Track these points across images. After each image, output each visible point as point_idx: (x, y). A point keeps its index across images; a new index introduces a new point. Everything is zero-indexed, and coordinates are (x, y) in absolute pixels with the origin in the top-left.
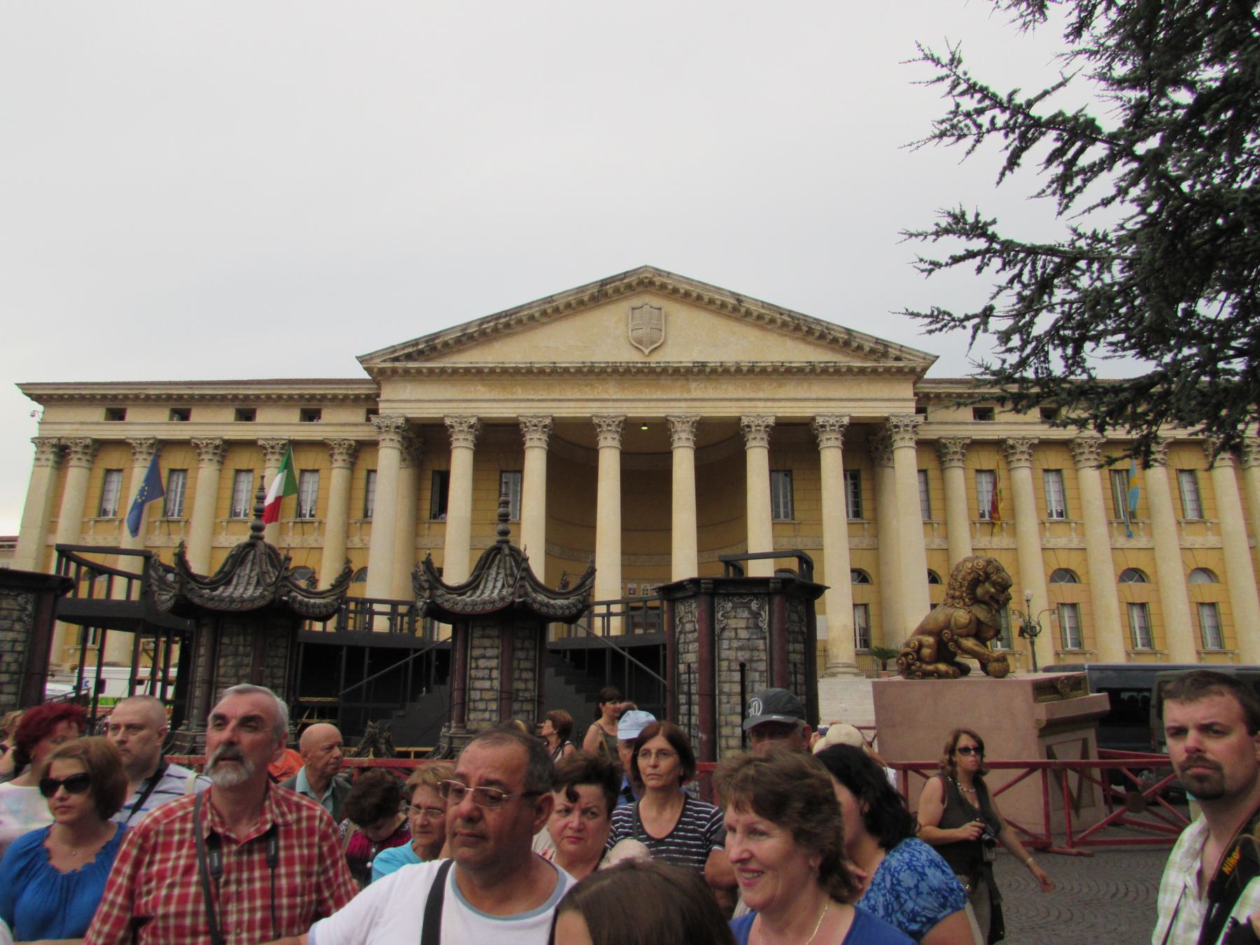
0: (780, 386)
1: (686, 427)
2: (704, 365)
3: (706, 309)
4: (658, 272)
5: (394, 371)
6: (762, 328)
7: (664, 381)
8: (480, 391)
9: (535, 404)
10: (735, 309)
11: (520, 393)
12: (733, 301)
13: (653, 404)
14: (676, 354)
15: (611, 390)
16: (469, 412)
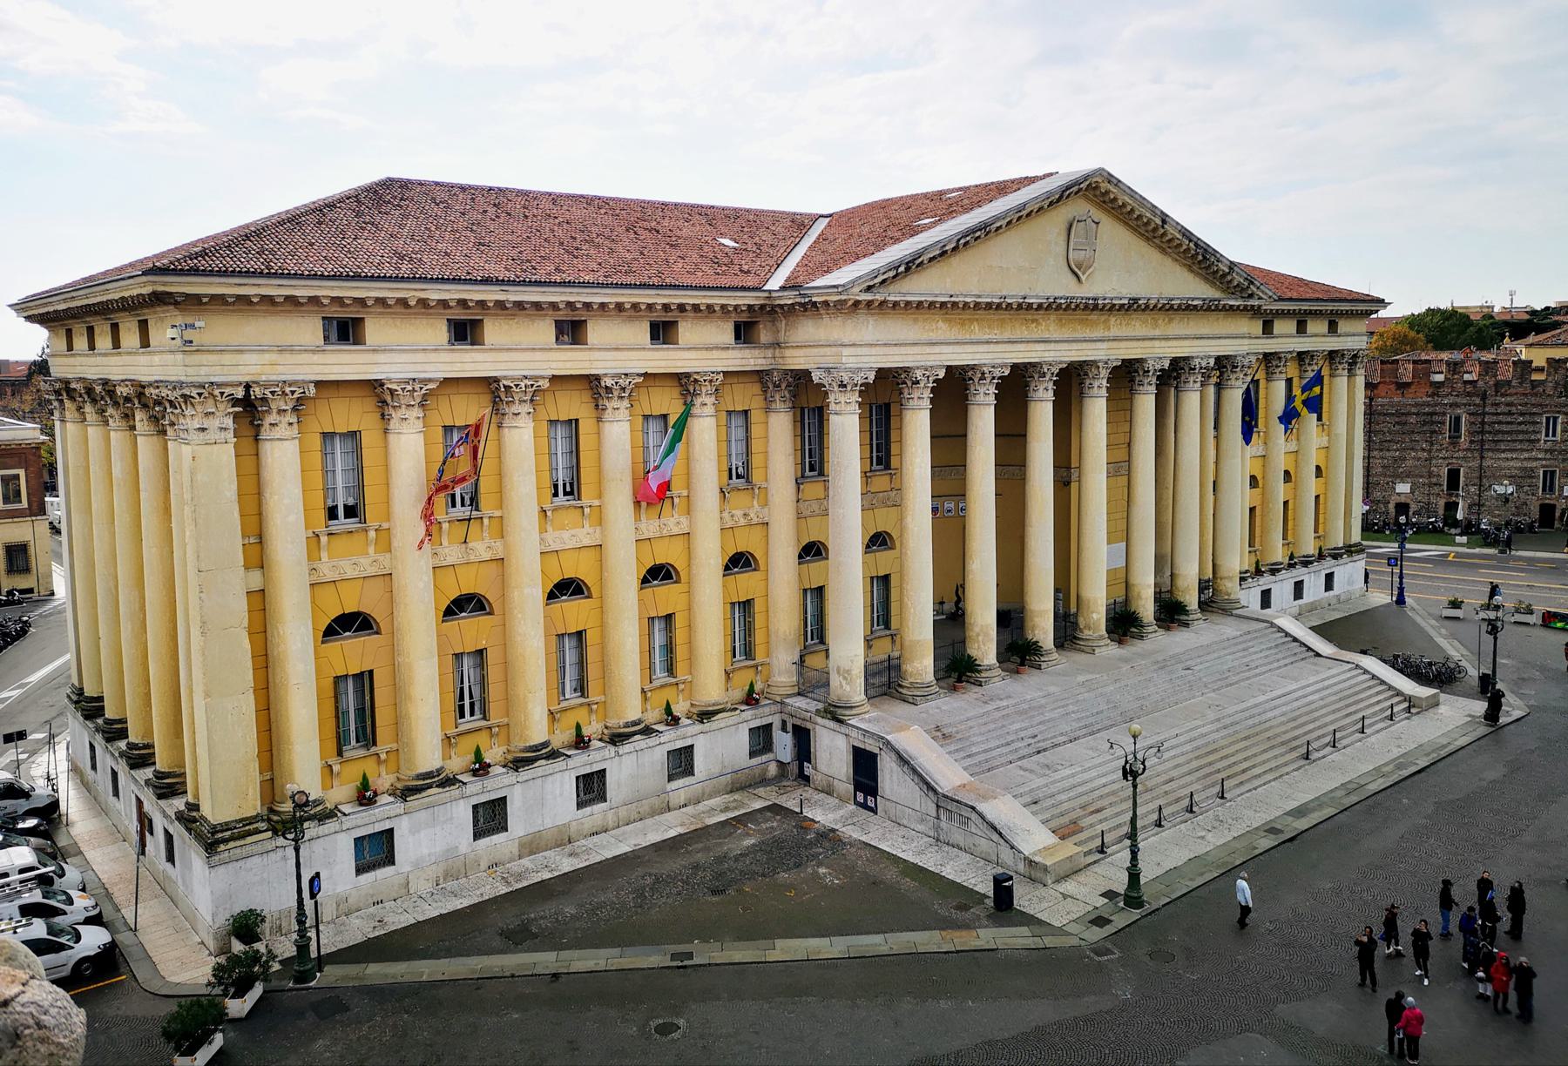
0: (1171, 320)
1: (1104, 373)
2: (1136, 300)
3: (1126, 224)
4: (1110, 178)
5: (869, 303)
6: (1163, 251)
7: (1094, 316)
8: (940, 328)
9: (992, 347)
10: (1155, 230)
11: (977, 332)
12: (1159, 222)
13: (1084, 345)
14: (1105, 284)
15: (1049, 327)
16: (931, 360)
